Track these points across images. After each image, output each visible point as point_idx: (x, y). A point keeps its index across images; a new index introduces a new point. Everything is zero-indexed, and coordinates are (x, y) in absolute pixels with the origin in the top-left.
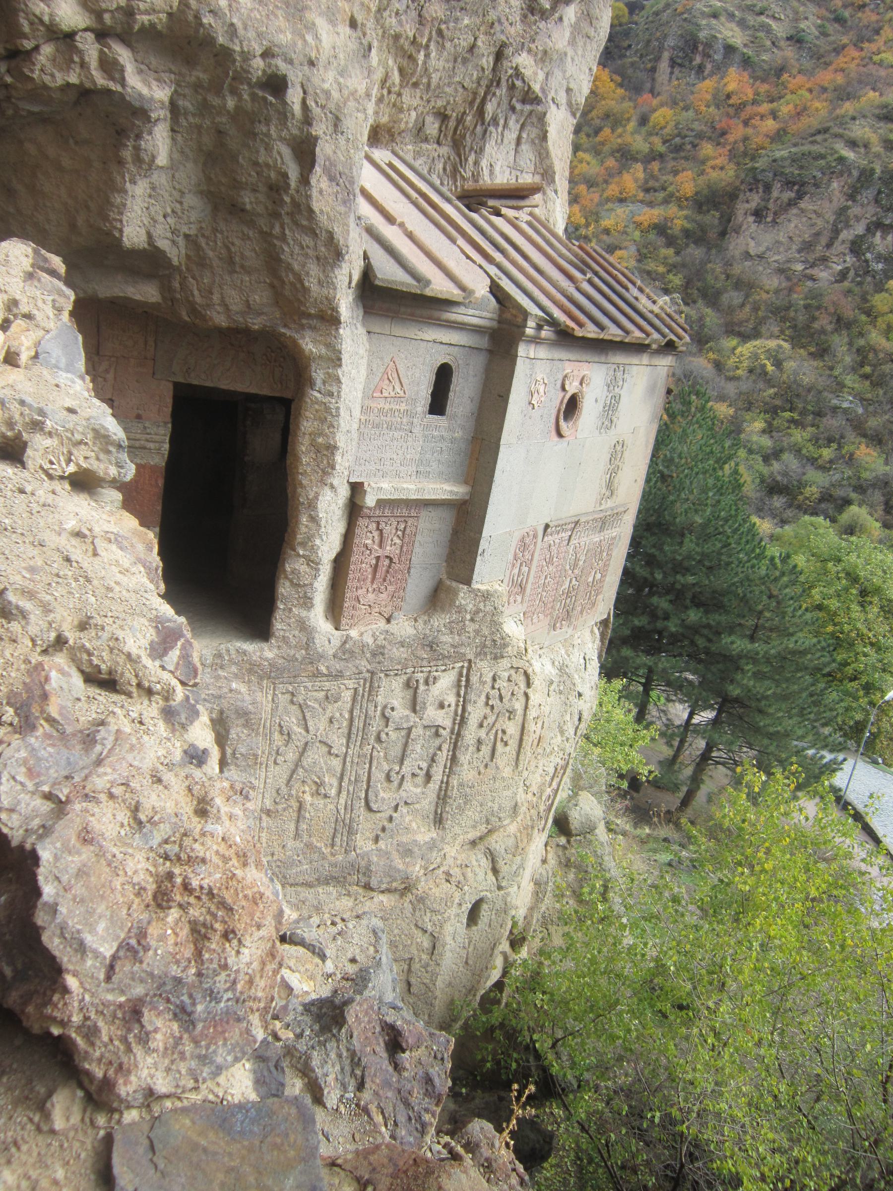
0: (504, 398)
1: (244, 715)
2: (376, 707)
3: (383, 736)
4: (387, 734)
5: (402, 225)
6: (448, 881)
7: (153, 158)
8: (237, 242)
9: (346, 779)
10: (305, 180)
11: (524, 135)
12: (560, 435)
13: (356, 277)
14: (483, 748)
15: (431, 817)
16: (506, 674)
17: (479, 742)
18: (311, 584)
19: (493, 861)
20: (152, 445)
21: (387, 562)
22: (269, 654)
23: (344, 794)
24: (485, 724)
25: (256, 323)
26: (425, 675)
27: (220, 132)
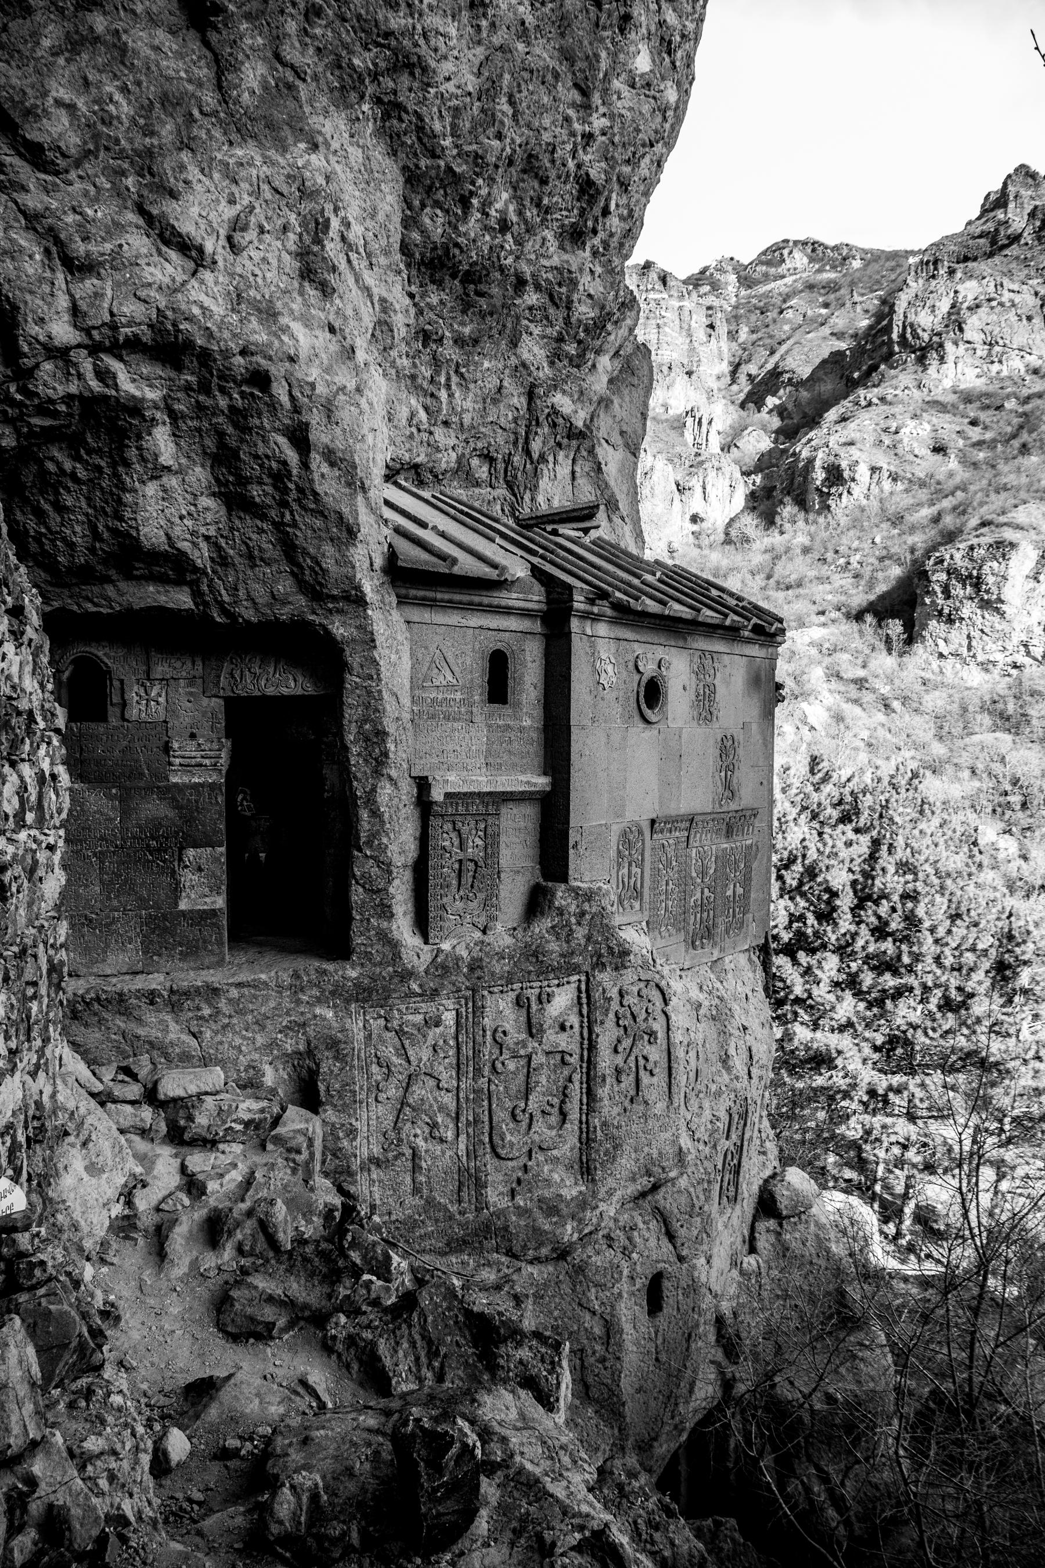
0: (567, 678)
3: (499, 1066)
5: (434, 528)
7: (156, 456)
8: (254, 536)
9: (463, 1119)
10: (305, 465)
11: (577, 469)
12: (647, 722)
13: (379, 562)
14: (623, 1077)
16: (635, 989)
17: (618, 1071)
19: (666, 1222)
20: (207, 762)
22: (353, 974)
23: (463, 1138)
24: (620, 1049)
25: (284, 613)
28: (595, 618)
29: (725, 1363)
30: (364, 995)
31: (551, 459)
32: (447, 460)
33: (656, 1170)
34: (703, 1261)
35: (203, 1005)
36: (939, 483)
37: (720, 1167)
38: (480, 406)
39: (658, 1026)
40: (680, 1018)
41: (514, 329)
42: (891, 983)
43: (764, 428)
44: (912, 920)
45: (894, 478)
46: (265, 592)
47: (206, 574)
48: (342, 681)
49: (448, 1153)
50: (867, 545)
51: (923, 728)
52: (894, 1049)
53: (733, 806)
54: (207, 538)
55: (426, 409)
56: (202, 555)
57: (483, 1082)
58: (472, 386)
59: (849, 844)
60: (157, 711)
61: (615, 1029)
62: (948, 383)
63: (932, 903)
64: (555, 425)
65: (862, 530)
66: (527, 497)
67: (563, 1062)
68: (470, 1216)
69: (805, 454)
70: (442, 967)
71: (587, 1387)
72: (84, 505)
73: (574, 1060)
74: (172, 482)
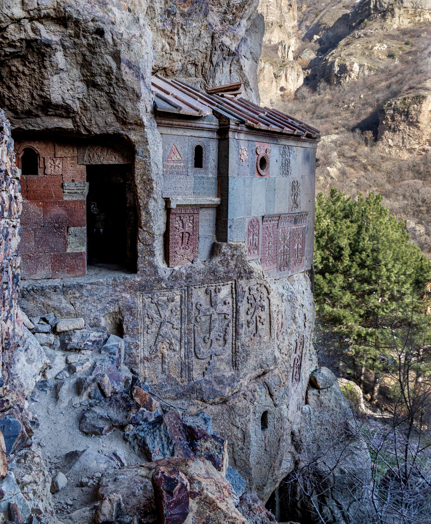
1: (130, 309)
2: (192, 304)
3: (198, 319)
4: (200, 318)
9: (183, 341)
10: (119, 68)
14: (250, 325)
15: (231, 363)
16: (256, 288)
17: (248, 322)
18: (152, 244)
22: (138, 279)
23: (183, 349)
24: (249, 313)
25: (111, 130)
26: (214, 287)
28: (239, 132)
29: (295, 453)
30: (143, 288)
31: (221, 65)
32: (178, 66)
33: (265, 366)
34: (285, 406)
35: (76, 292)
36: (390, 71)
37: (292, 365)
38: (192, 42)
40: (275, 301)
41: (206, 9)
42: (367, 288)
43: (312, 49)
44: (376, 261)
45: (370, 69)
46: (102, 122)
47: (78, 113)
48: (134, 158)
50: (357, 99)
51: (381, 178)
52: (369, 317)
53: (297, 211)
54: (79, 99)
55: (169, 44)
56: (76, 106)
57: (191, 326)
58: (188, 34)
59: (348, 227)
60: (59, 171)
61: (247, 304)
62: (395, 26)
63: (386, 253)
64: (223, 50)
65: (355, 92)
66: (211, 81)
67: (225, 318)
68: (186, 383)
69: (330, 60)
70: (175, 277)
71: (235, 460)
72: (28, 84)
73: (230, 317)
74: (64, 75)
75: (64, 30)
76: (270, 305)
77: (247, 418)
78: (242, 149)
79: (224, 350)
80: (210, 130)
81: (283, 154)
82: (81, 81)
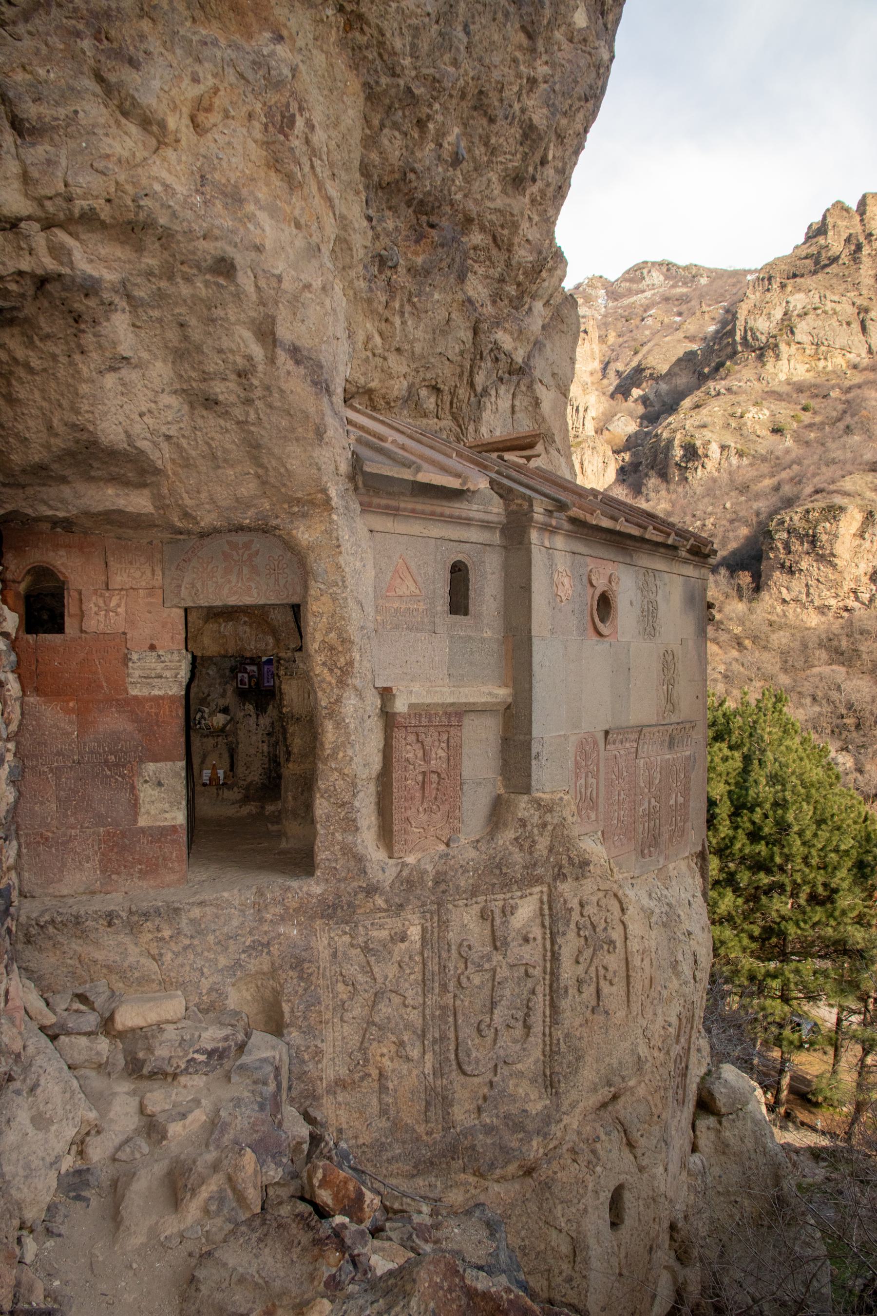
3: (464, 980)
6: (574, 1161)
7: (114, 344)
8: (218, 436)
9: (429, 1036)
10: (272, 360)
11: (517, 403)
12: (600, 634)
13: (344, 468)
14: (585, 987)
15: (540, 1080)
16: (594, 899)
17: (580, 982)
21: (435, 776)
22: (318, 890)
23: (429, 1056)
24: (581, 960)
27: (182, 325)
33: (617, 1079)
34: (661, 1169)
39: (616, 935)
40: (636, 928)
47: (168, 477)
49: (415, 1072)
54: (168, 438)
56: (161, 456)
57: (449, 999)
60: (116, 622)
67: (527, 975)
68: (437, 1136)
70: (409, 883)
72: (37, 395)
73: (537, 972)
74: (130, 375)
75: (133, 256)
76: (626, 938)
77: (581, 1206)
78: (558, 570)
79: (524, 1050)
80: (486, 526)
81: (644, 589)
82: (175, 392)
